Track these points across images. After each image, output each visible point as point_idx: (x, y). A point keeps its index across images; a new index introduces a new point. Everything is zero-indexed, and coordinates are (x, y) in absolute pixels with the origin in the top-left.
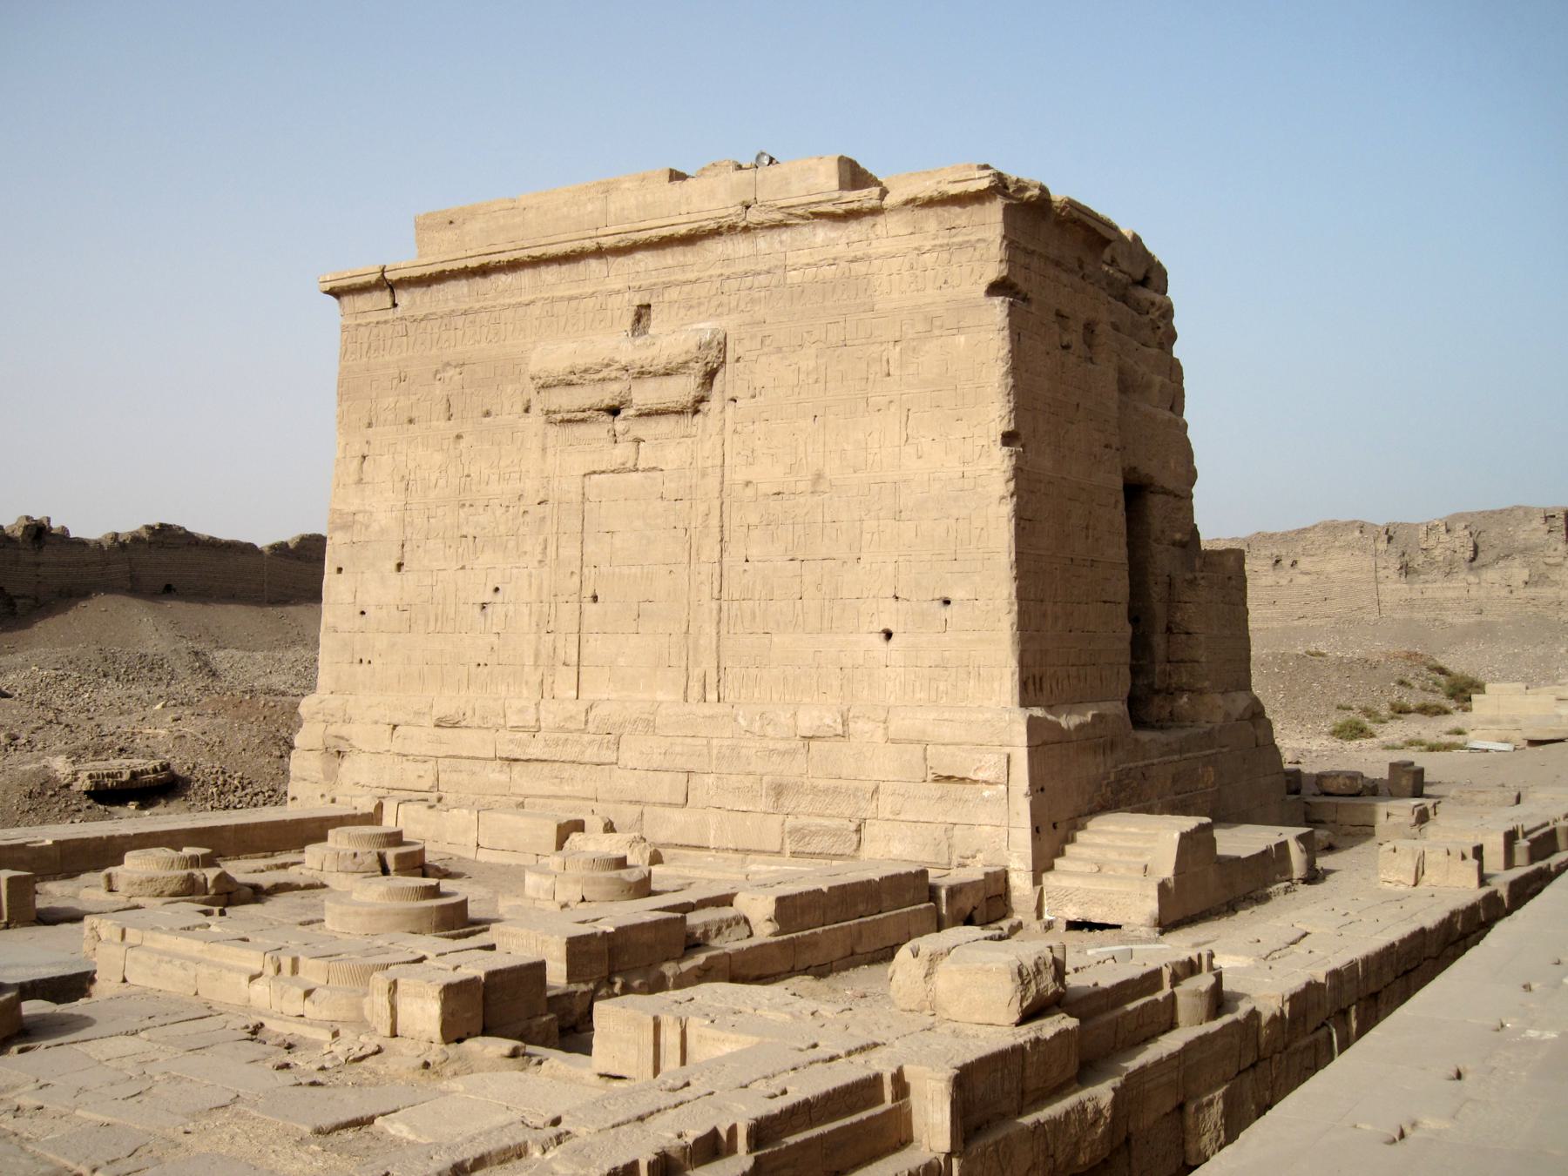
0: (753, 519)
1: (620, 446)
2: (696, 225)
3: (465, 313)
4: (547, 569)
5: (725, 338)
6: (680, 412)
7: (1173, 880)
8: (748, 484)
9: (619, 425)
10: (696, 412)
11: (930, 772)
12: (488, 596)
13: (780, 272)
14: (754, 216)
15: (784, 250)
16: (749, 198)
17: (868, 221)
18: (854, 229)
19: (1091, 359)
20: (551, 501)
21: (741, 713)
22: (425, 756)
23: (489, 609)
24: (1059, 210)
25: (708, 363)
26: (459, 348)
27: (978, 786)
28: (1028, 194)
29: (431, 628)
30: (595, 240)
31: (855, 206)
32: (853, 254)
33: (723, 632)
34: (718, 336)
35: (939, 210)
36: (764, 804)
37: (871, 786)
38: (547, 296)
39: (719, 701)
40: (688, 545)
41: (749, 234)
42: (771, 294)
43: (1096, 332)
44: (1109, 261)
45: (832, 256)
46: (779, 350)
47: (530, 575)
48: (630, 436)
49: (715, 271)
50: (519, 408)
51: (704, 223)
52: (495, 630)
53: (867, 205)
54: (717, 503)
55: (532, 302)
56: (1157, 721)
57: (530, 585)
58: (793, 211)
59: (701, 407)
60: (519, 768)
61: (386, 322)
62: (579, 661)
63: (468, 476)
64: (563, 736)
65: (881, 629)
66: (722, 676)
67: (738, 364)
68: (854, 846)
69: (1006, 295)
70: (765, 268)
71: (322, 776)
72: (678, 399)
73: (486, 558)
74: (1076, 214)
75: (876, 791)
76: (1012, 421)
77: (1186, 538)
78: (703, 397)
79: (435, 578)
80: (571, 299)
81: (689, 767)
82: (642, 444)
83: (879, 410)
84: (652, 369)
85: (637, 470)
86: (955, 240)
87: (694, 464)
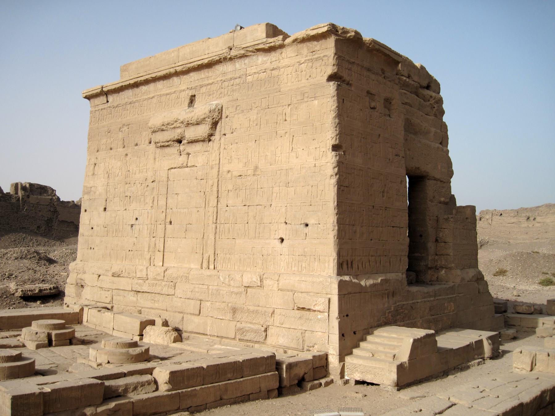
0: (230, 187)
1: (182, 156)
2: (211, 59)
3: (130, 103)
4: (154, 210)
5: (222, 107)
6: (203, 141)
7: (407, 363)
8: (229, 172)
9: (182, 147)
10: (210, 140)
11: (295, 305)
12: (133, 222)
13: (244, 77)
14: (233, 53)
15: (246, 67)
16: (231, 45)
17: (279, 51)
18: (274, 56)
19: (390, 115)
20: (156, 181)
21: (221, 275)
22: (108, 288)
23: (134, 227)
24: (368, 45)
25: (214, 118)
26: (128, 118)
27: (316, 313)
28: (349, 35)
29: (114, 235)
30: (174, 68)
31: (272, 44)
32: (272, 67)
33: (217, 238)
34: (219, 107)
35: (308, 44)
36: (229, 316)
37: (271, 310)
38: (158, 94)
39: (214, 269)
40: (205, 199)
41: (232, 61)
42: (240, 87)
43: (392, 103)
44: (407, 76)
45: (264, 68)
46: (243, 111)
47: (148, 213)
48: (185, 152)
49: (219, 79)
50: (147, 142)
51: (214, 58)
53: (277, 43)
54: (216, 180)
55: (153, 97)
56: (430, 281)
57: (148, 217)
58: (248, 49)
59: (211, 139)
60: (140, 295)
61: (104, 109)
62: (164, 250)
63: (129, 171)
64: (155, 282)
66: (216, 257)
67: (226, 119)
68: (264, 338)
69: (336, 81)
70: (238, 76)
71: (75, 295)
73: (134, 205)
74: (377, 47)
75: (273, 312)
76: (338, 140)
77: (447, 200)
78: (212, 134)
79: (116, 214)
80: (167, 94)
81: (201, 298)
82: (190, 155)
83: (281, 137)
84: (191, 122)
85: (188, 167)
86: (314, 57)
87: (208, 164)
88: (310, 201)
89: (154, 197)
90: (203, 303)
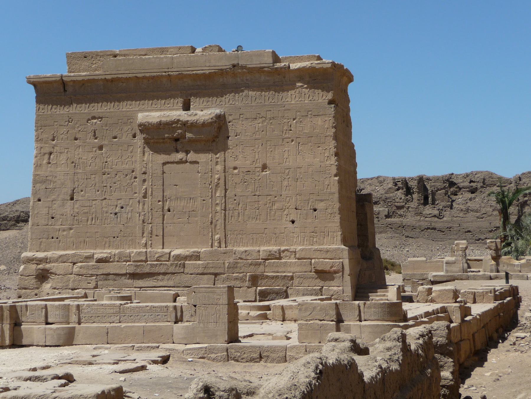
10: (214, 141)
50: (130, 136)
52: (122, 223)
63: (106, 162)
65: (291, 219)
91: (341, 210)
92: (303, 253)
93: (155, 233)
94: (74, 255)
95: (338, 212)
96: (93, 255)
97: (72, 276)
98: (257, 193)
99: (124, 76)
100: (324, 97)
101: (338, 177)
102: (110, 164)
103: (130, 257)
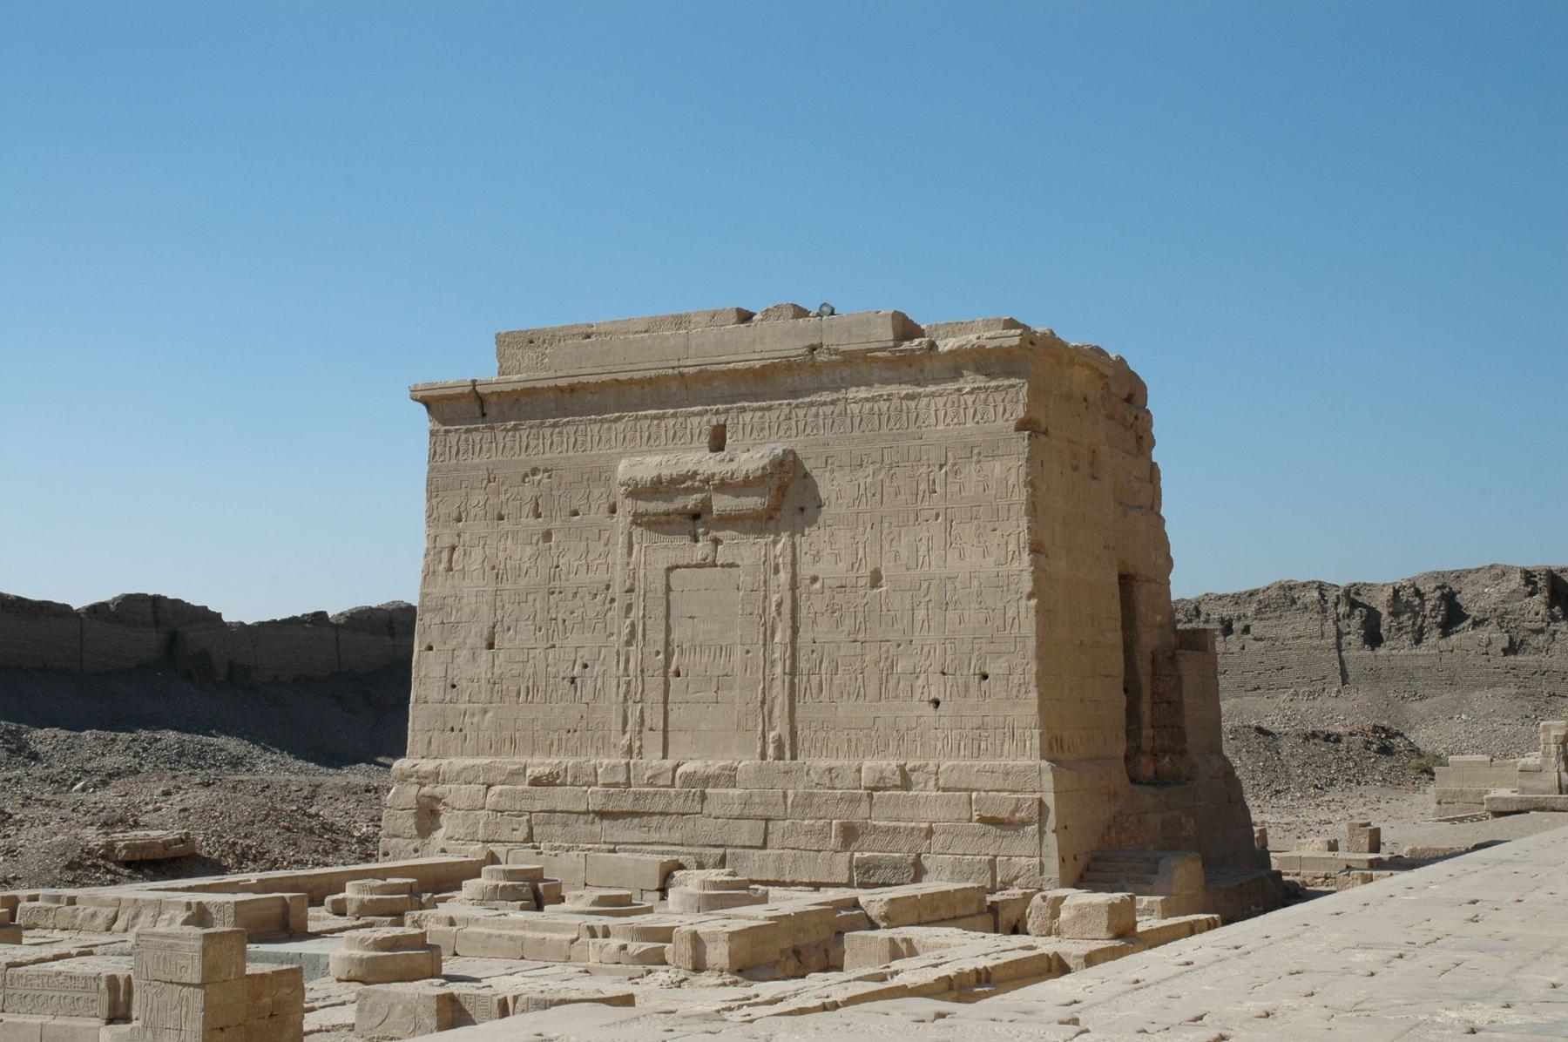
1: (700, 544)
10: (771, 518)
26: (547, 455)
47: (618, 653)
54: (788, 594)
57: (618, 662)
63: (557, 567)
65: (932, 697)
72: (752, 507)
73: (574, 639)
85: (716, 566)
88: (990, 636)
89: (633, 625)
90: (770, 825)
91: (1041, 679)
92: (955, 776)
93: (648, 723)
94: (487, 769)
95: (1034, 683)
96: (525, 769)
97: (483, 812)
98: (861, 637)
99: (592, 379)
100: (1007, 415)
101: (1036, 600)
102: (565, 570)
103: (596, 775)
